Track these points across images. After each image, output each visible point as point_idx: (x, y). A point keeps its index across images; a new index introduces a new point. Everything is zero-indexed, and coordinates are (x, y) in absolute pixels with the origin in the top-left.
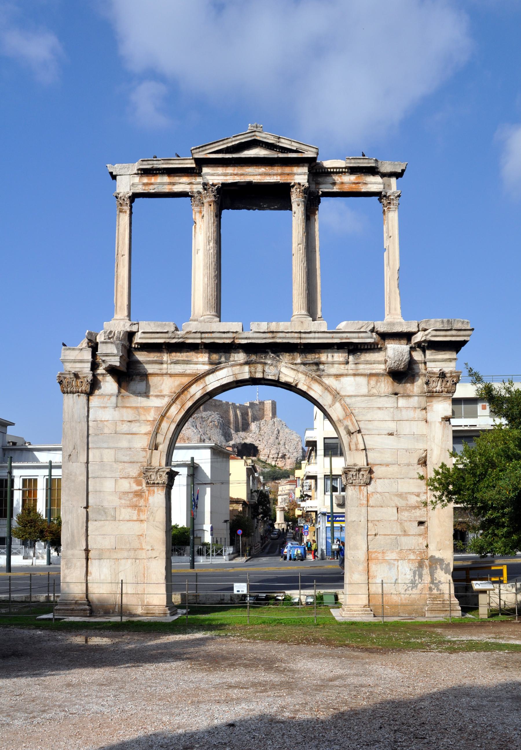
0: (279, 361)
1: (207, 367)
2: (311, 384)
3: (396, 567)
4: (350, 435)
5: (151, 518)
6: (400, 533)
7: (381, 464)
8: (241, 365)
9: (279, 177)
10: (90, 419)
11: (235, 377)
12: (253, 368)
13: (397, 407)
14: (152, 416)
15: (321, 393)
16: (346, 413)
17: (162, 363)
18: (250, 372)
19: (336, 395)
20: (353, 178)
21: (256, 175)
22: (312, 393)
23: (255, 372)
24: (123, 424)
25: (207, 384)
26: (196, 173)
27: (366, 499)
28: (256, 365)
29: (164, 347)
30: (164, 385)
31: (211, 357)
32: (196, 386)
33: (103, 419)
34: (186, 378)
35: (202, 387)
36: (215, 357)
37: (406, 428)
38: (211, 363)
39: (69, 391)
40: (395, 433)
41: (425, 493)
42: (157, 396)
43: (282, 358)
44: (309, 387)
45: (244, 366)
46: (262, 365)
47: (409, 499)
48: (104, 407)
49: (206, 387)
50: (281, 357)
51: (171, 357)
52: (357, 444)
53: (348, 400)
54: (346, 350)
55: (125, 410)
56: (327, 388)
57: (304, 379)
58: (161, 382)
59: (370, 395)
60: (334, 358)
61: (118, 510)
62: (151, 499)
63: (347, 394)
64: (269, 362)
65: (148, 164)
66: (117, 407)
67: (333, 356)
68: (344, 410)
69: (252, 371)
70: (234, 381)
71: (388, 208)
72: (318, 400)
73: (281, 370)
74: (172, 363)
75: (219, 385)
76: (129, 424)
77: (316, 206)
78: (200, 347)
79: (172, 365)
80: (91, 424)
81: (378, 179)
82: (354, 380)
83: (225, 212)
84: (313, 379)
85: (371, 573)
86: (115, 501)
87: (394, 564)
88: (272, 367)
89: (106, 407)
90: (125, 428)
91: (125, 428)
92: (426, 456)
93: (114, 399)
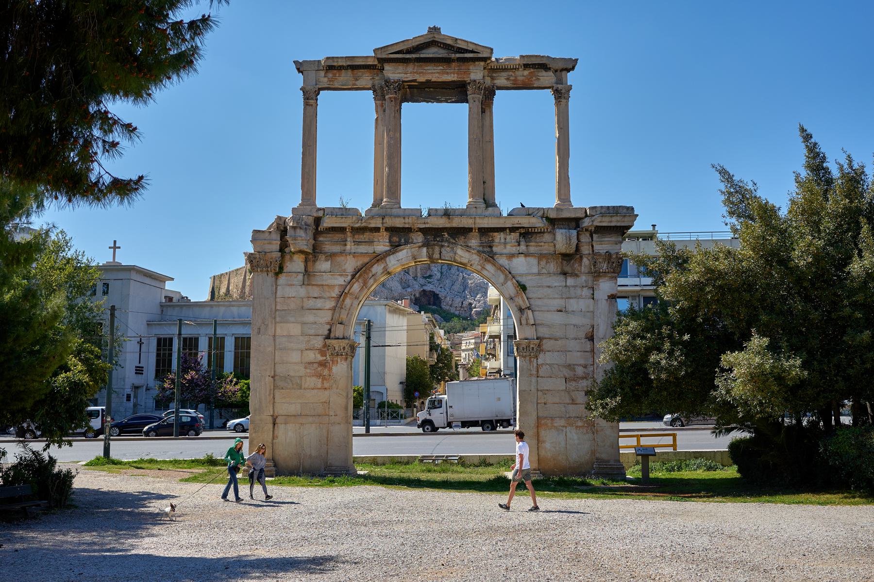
0: (454, 243)
1: (388, 248)
3: (564, 433)
4: (521, 311)
5: (334, 386)
6: (568, 402)
7: (550, 338)
8: (420, 247)
9: (456, 75)
10: (277, 296)
13: (566, 286)
14: (335, 293)
15: (493, 272)
19: (509, 274)
20: (526, 73)
21: (434, 73)
22: (485, 273)
24: (309, 300)
26: (378, 69)
27: (535, 370)
29: (348, 230)
30: (347, 264)
33: (290, 296)
35: (383, 266)
36: (395, 239)
37: (573, 305)
39: (259, 270)
40: (564, 309)
41: (591, 365)
42: (341, 275)
44: (483, 268)
47: (577, 370)
48: (291, 285)
52: (527, 319)
53: (519, 279)
55: (310, 287)
56: (500, 268)
57: (478, 260)
59: (539, 274)
60: (507, 240)
61: (303, 379)
62: (334, 369)
64: (446, 244)
65: (334, 61)
66: (303, 284)
71: (559, 101)
76: (314, 299)
77: (491, 100)
78: (381, 231)
80: (278, 300)
81: (551, 73)
82: (526, 261)
83: (405, 105)
84: (486, 260)
85: (541, 439)
86: (302, 371)
87: (563, 430)
89: (294, 285)
90: (311, 303)
91: (311, 303)
92: (593, 331)
93: (300, 277)
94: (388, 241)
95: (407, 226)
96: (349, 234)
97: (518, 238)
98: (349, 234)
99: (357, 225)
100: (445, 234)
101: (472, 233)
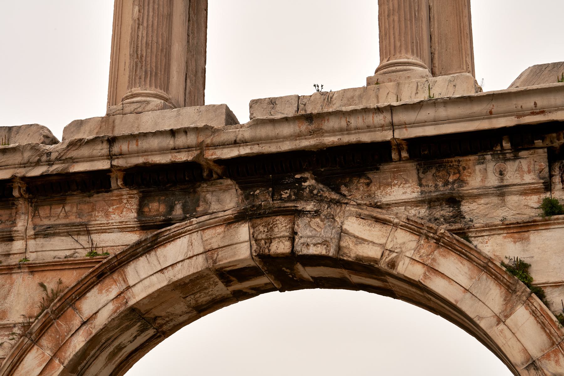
0: (338, 203)
1: (132, 238)
2: (434, 260)
11: (212, 258)
12: (261, 229)
15: (464, 281)
16: (550, 335)
17: (11, 239)
18: (256, 240)
23: (270, 240)
25: (131, 283)
28: (270, 220)
29: (16, 193)
30: (11, 298)
31: (146, 209)
32: (100, 291)
34: (75, 273)
35: (114, 292)
38: (144, 227)
43: (346, 193)
45: (236, 225)
46: (288, 218)
49: (128, 294)
50: (344, 190)
51: (37, 221)
54: (541, 151)
57: (413, 245)
58: (7, 286)
60: (507, 177)
63: (552, 280)
64: (310, 207)
67: (501, 173)
68: (543, 326)
69: (259, 237)
70: (208, 269)
72: (459, 305)
73: (344, 227)
74: (36, 236)
75: (165, 283)
78: (113, 185)
79: (40, 241)
84: (441, 243)
88: (318, 220)
94: (134, 215)
95: (183, 157)
96: (22, 205)
97: (544, 164)
98: (22, 205)
99: (37, 172)
100: (307, 175)
101: (392, 165)
